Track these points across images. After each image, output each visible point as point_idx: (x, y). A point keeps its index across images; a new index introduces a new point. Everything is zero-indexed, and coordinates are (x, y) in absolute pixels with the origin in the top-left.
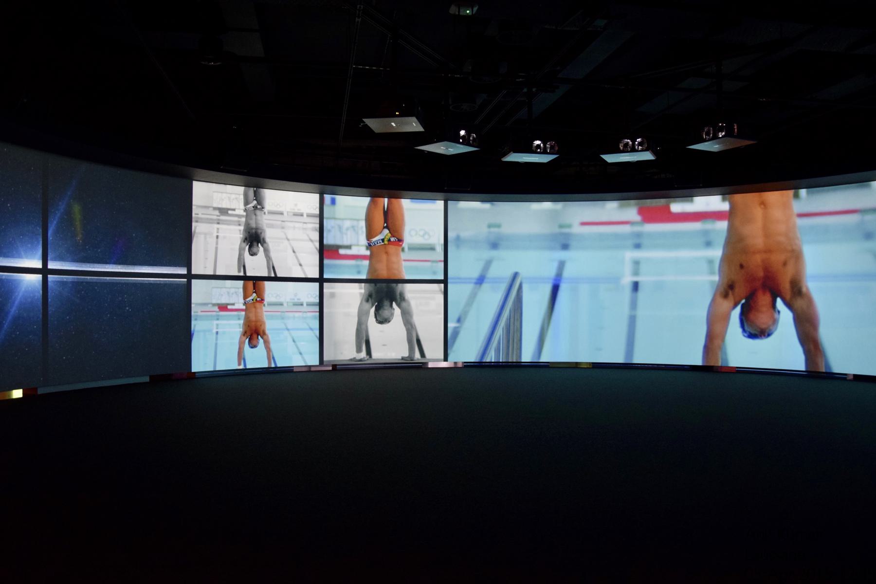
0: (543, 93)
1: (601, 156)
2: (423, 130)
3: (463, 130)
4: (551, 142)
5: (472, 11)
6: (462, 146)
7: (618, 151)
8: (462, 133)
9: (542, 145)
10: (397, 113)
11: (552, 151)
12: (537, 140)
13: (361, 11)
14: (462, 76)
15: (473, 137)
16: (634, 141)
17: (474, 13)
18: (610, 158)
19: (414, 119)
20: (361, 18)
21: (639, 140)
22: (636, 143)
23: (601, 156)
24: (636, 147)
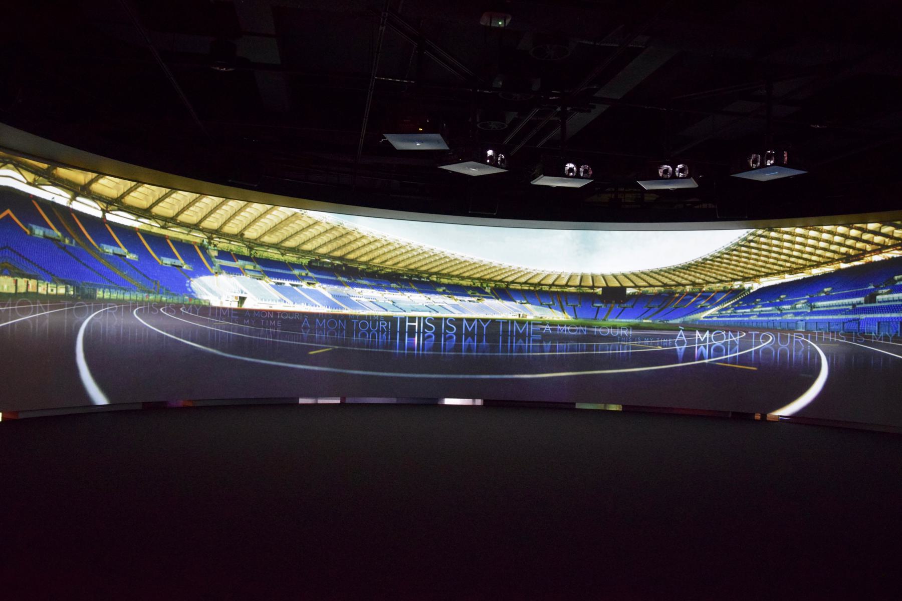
0: (578, 113)
2: (448, 148)
3: (491, 149)
4: (585, 165)
5: (505, 22)
6: (490, 167)
7: (655, 177)
9: (575, 169)
10: (420, 129)
13: (386, 19)
15: (502, 158)
16: (674, 168)
17: (506, 24)
18: (647, 186)
19: (438, 136)
20: (385, 27)
21: (680, 166)
22: (677, 169)
24: (677, 174)
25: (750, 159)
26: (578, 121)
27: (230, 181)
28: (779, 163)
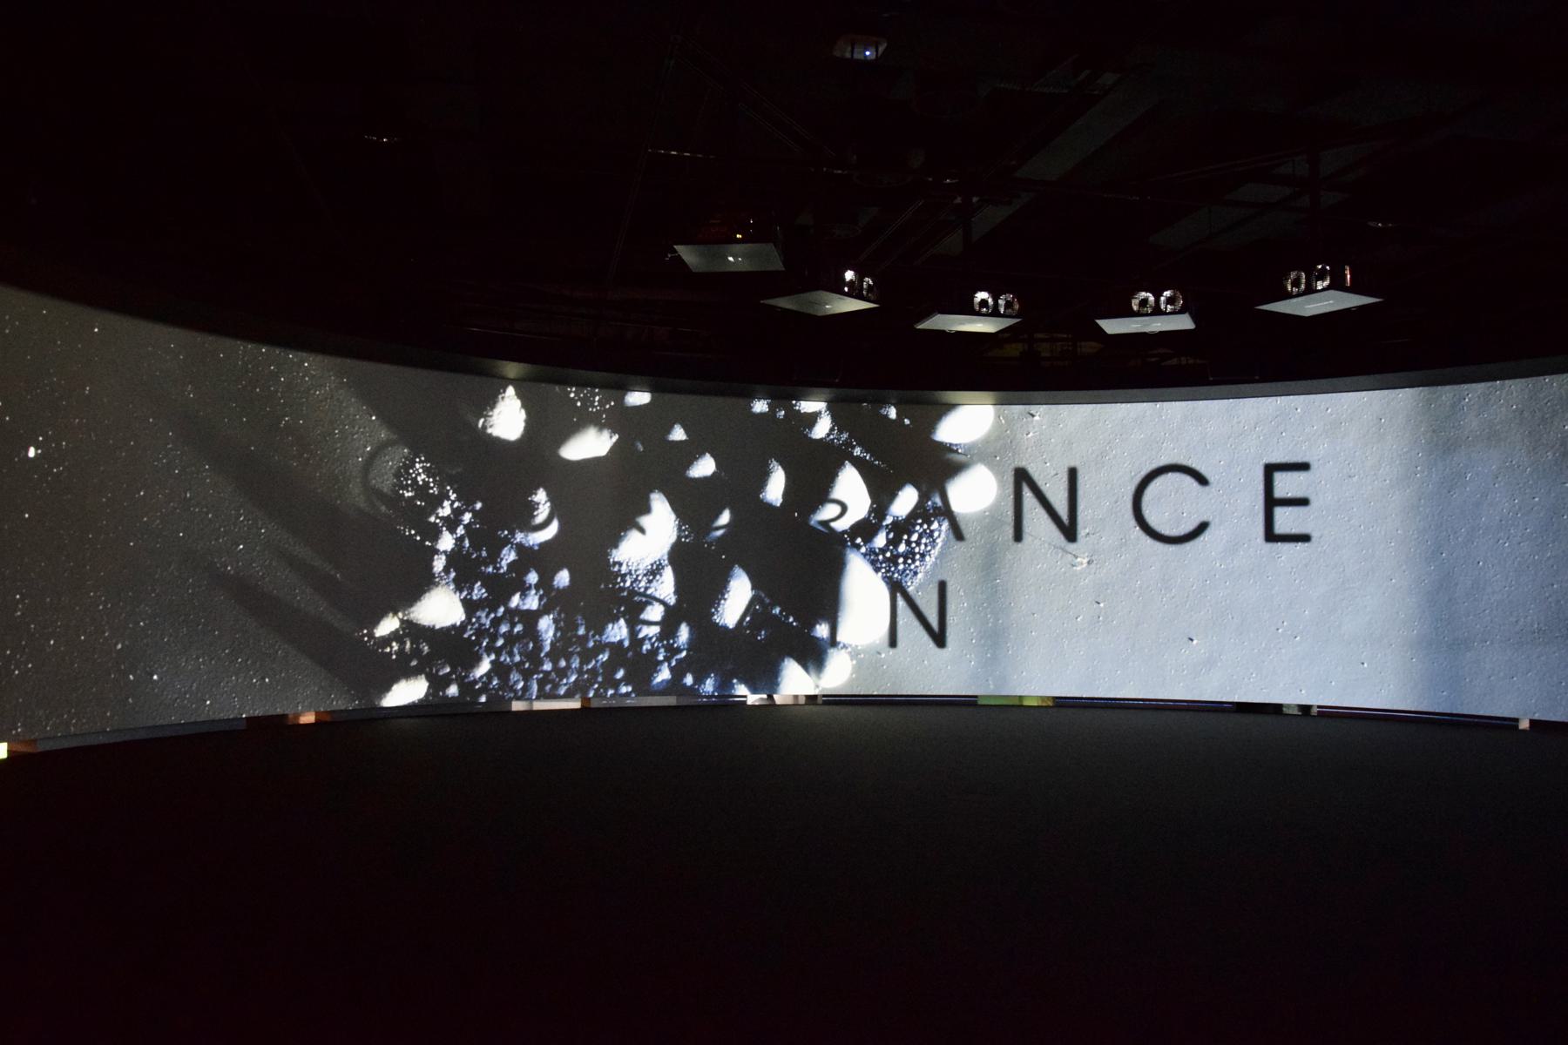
4: (1007, 295)
5: (877, 51)
9: (990, 301)
10: (738, 236)
14: (846, 172)
16: (1157, 297)
18: (1112, 326)
21: (1167, 293)
22: (1162, 299)
23: (1098, 321)
24: (1163, 307)
25: (1287, 279)
26: (990, 217)
28: (1337, 285)
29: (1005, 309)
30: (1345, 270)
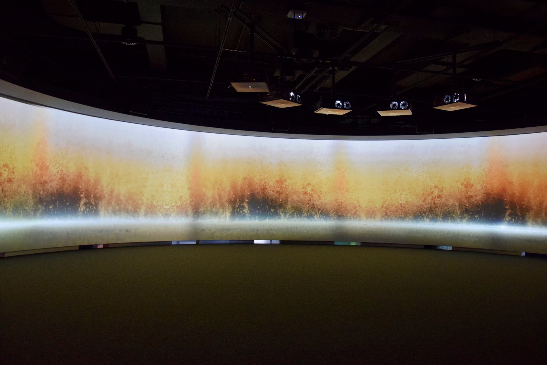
0: (341, 71)
1: (378, 112)
4: (347, 102)
6: (292, 103)
7: (388, 109)
8: (292, 94)
9: (341, 104)
11: (347, 107)
12: (338, 100)
13: (233, 13)
14: (291, 58)
16: (399, 103)
17: (304, 17)
18: (383, 114)
19: (264, 84)
20: (232, 18)
21: (402, 102)
22: (401, 104)
23: (378, 112)
24: (401, 107)
26: (341, 75)
27: (131, 112)
28: (462, 100)
29: (346, 107)
30: (464, 95)
